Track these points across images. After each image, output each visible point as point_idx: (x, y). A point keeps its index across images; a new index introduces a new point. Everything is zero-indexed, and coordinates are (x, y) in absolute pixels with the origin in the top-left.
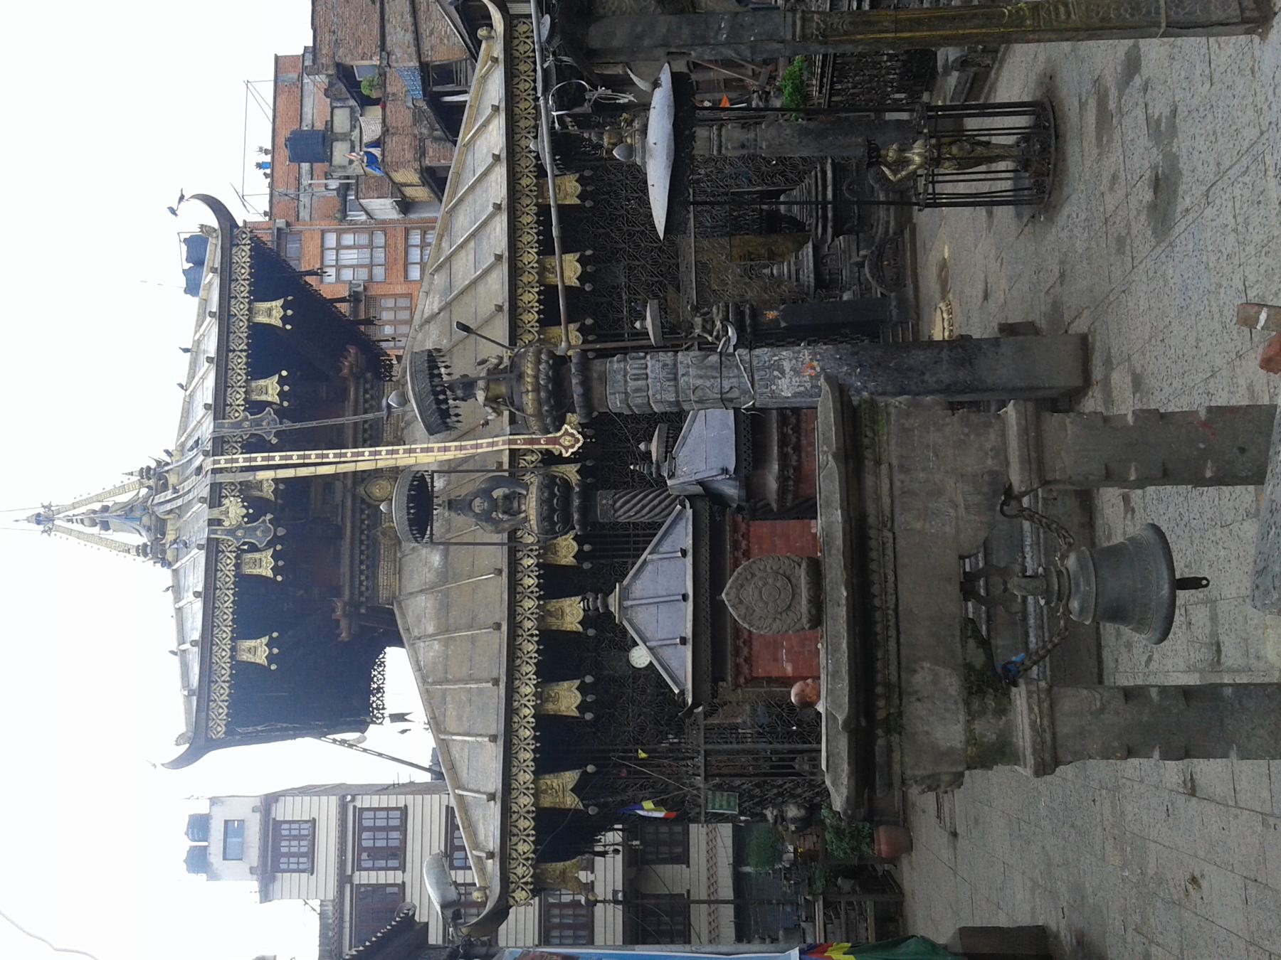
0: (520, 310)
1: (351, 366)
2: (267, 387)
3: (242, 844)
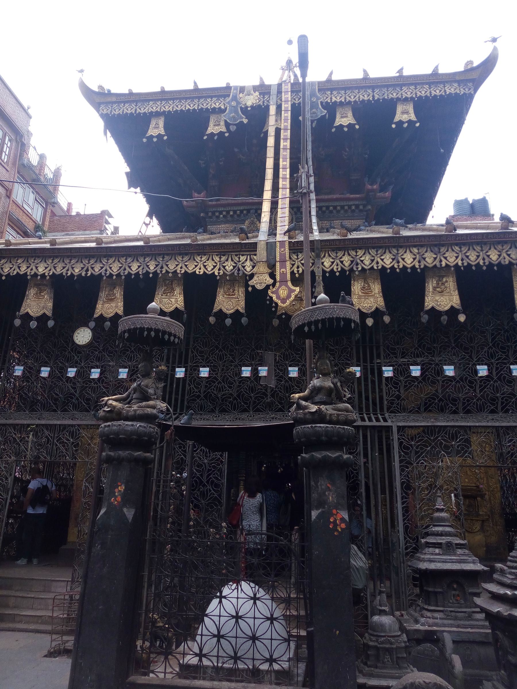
0: (395, 251)
1: (372, 190)
2: (346, 117)
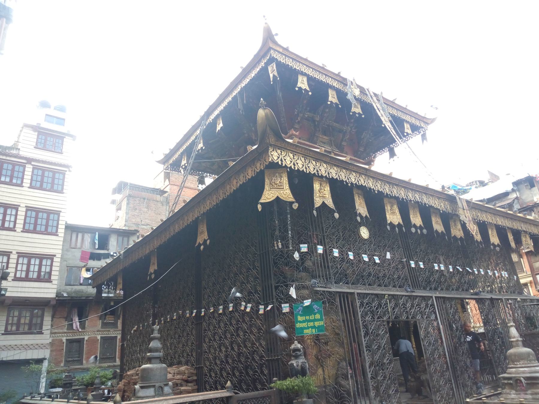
3: (53, 123)
